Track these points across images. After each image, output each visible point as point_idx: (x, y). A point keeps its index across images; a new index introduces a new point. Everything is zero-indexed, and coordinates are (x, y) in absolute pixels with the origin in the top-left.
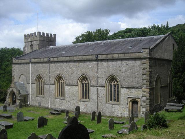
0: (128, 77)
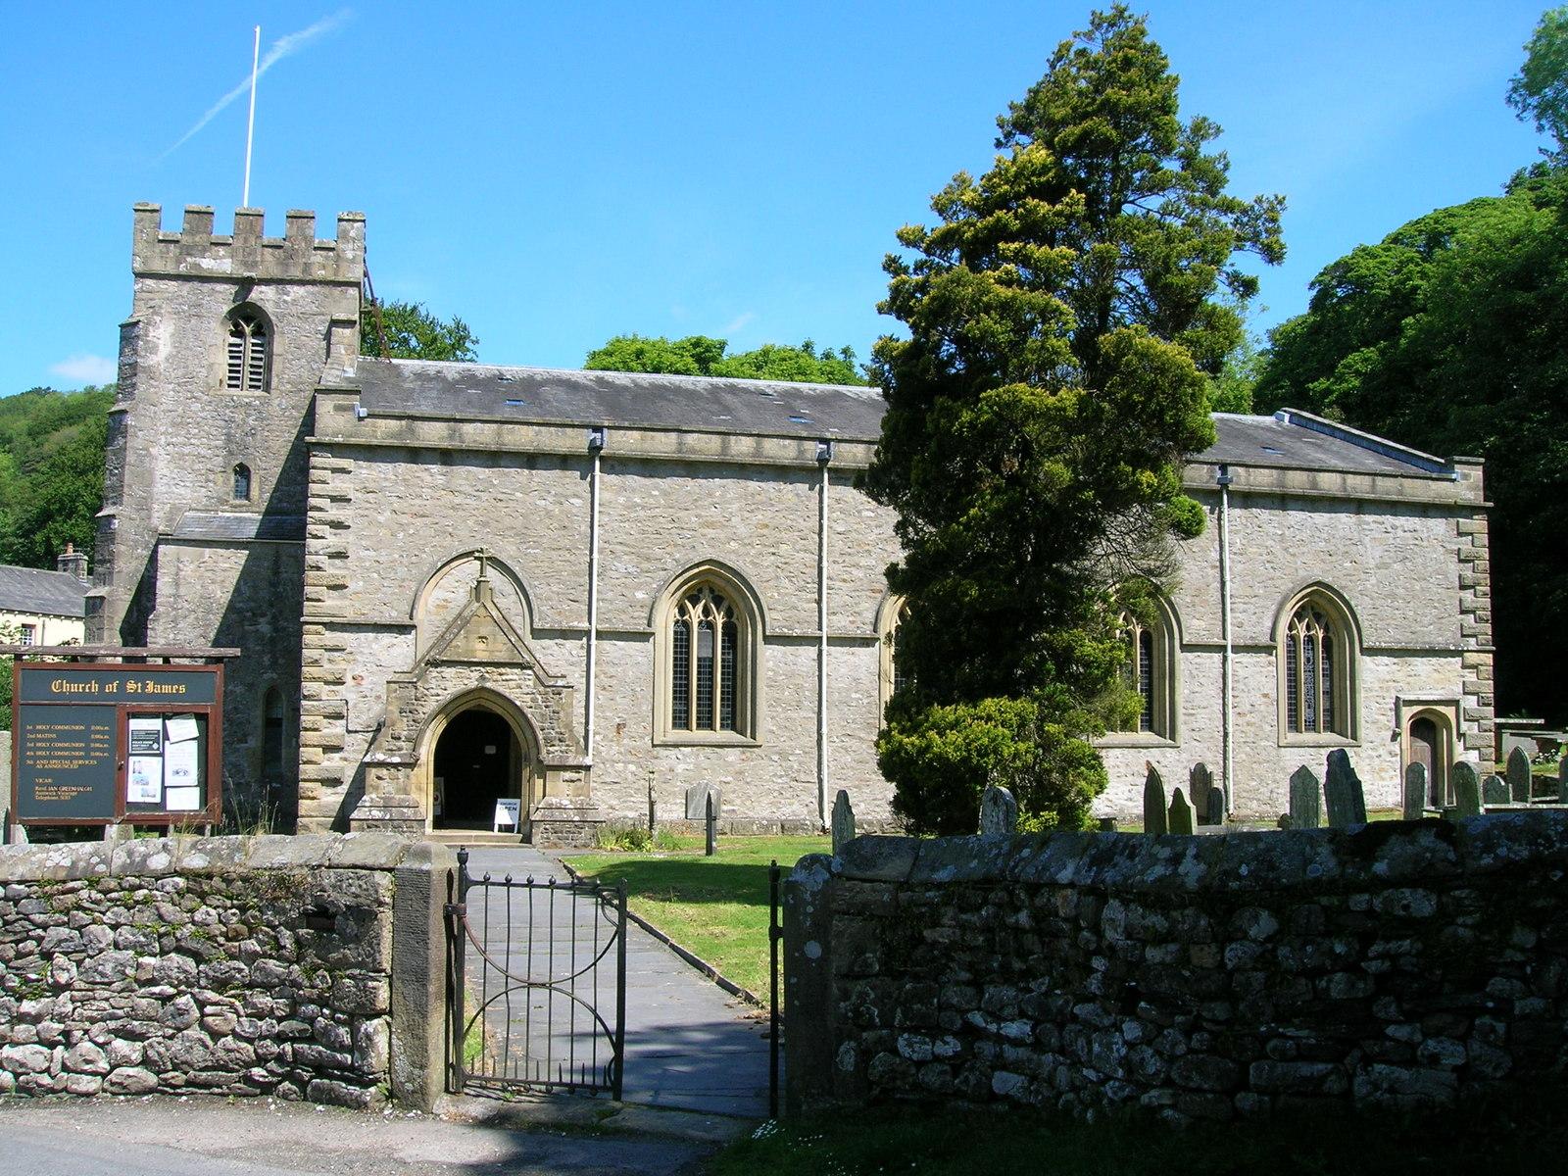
0: (1393, 596)
